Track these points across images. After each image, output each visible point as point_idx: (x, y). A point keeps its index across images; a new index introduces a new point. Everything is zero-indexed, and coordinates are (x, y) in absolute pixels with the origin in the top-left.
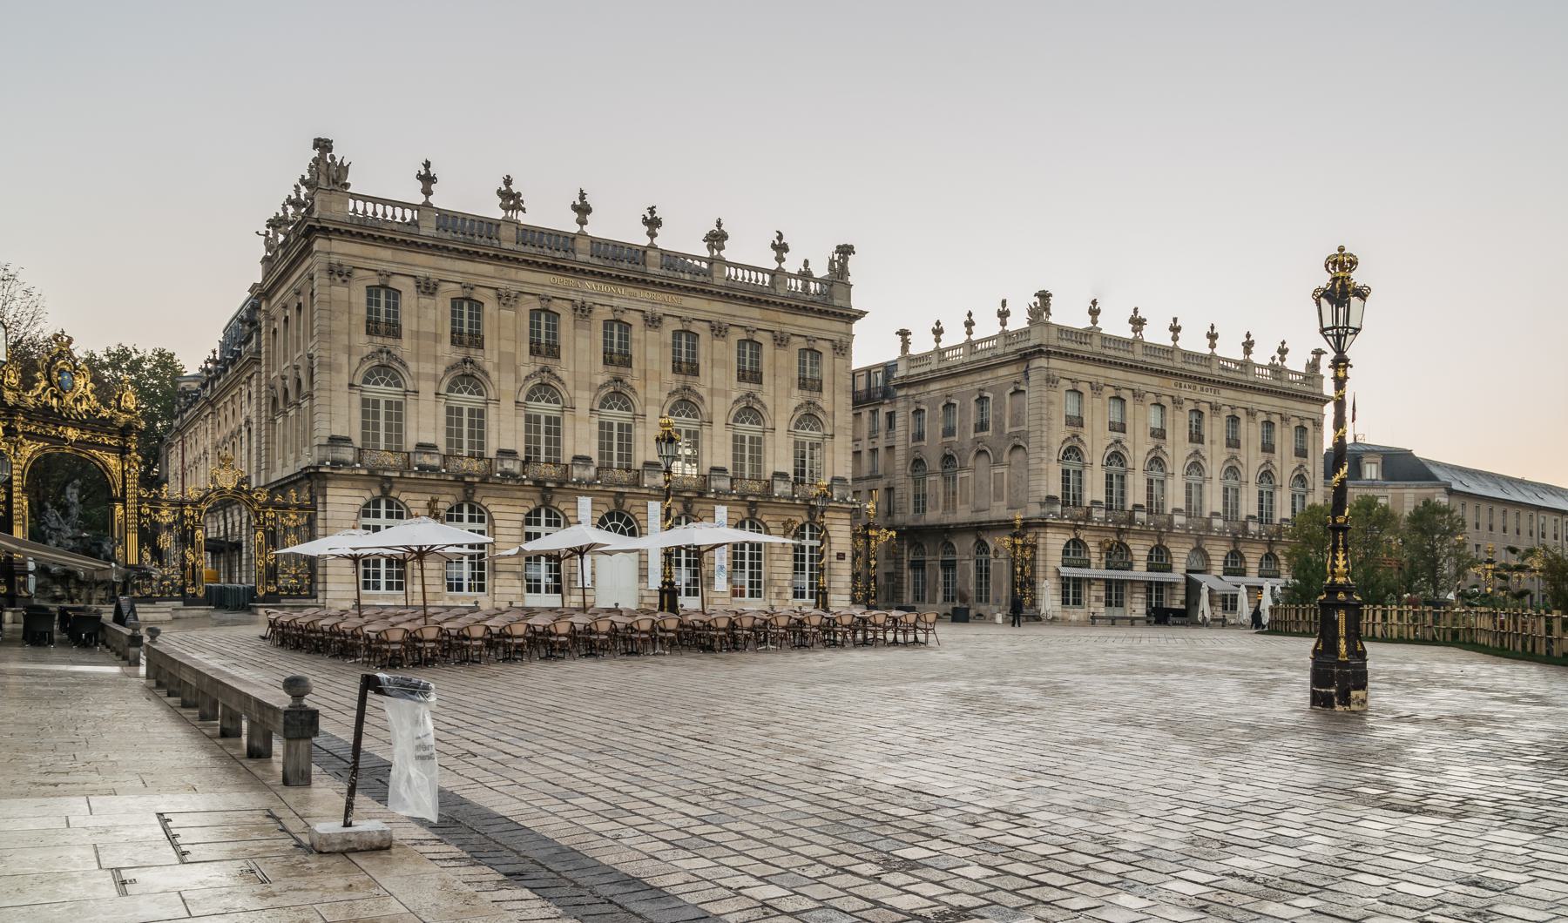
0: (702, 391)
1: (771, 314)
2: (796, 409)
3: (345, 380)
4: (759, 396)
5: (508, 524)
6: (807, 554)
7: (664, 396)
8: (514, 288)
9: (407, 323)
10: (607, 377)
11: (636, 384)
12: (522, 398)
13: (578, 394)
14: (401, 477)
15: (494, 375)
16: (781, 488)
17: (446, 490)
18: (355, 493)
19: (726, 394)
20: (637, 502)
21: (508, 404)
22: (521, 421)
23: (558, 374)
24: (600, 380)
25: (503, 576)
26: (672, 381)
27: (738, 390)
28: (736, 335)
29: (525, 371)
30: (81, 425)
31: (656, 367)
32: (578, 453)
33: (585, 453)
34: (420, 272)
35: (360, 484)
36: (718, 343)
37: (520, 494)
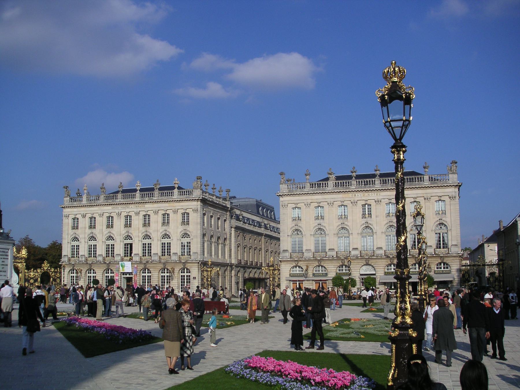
1: (172, 204)
2: (181, 232)
4: (168, 230)
6: (186, 278)
7: (140, 234)
9: (80, 226)
10: (125, 231)
12: (104, 240)
15: (98, 235)
21: (101, 242)
28: (161, 212)
34: (82, 213)
36: (156, 216)
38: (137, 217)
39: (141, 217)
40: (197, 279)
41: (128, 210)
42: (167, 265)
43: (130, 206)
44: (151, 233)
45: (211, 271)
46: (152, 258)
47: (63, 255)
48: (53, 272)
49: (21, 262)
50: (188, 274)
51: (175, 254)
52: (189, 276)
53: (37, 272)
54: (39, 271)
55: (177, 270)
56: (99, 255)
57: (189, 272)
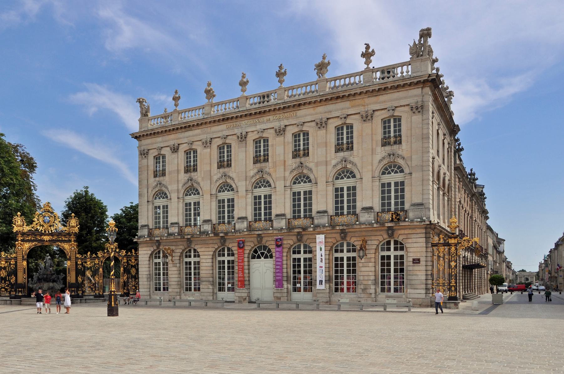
0: (311, 165)
3: (146, 199)
5: (206, 257)
7: (287, 174)
8: (208, 137)
10: (256, 171)
11: (271, 171)
12: (214, 192)
13: (239, 184)
14: (161, 239)
16: (365, 217)
17: (181, 243)
18: (148, 249)
19: (326, 163)
20: (270, 239)
21: (207, 197)
22: (214, 205)
23: (231, 175)
24: (252, 173)
25: (204, 283)
26: (292, 163)
27: (335, 158)
29: (215, 178)
30: (49, 235)
31: (282, 158)
32: (240, 216)
33: (244, 215)
35: (150, 245)
37: (211, 242)
38: (281, 139)
39: (289, 137)
40: (423, 263)
41: (260, 127)
42: (349, 235)
43: (265, 119)
44: (310, 170)
45: (456, 245)
46: (316, 222)
47: (140, 224)
48: (123, 257)
49: (70, 241)
50: (399, 253)
51: (368, 209)
52: (402, 257)
53: (98, 257)
55: (373, 243)
56: (205, 221)
57: (402, 249)
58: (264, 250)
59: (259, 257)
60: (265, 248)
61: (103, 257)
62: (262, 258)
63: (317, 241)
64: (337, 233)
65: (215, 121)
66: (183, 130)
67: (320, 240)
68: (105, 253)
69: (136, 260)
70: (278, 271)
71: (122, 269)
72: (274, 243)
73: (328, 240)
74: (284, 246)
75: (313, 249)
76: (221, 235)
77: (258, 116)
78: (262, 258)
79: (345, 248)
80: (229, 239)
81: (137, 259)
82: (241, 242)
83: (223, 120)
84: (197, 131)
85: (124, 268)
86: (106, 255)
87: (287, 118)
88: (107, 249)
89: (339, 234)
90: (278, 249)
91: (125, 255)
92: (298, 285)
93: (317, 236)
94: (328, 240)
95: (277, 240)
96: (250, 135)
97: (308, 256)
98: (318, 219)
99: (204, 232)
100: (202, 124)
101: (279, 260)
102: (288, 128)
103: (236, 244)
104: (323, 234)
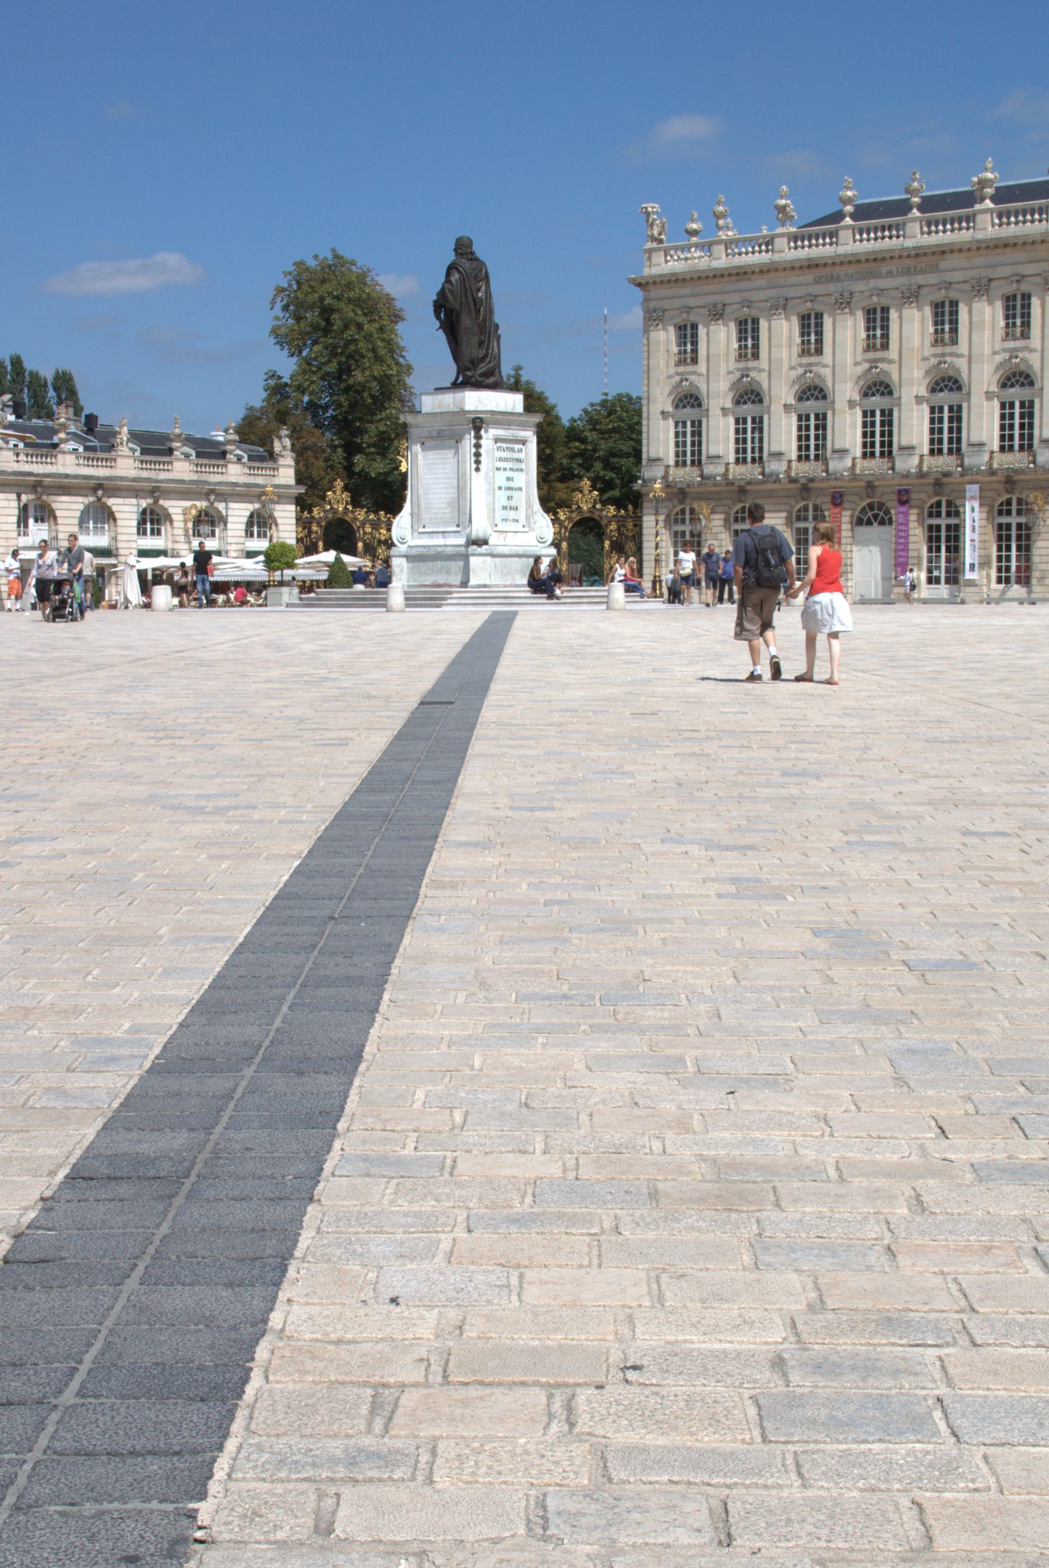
14: (688, 486)
34: (711, 299)
46: (967, 461)
47: (644, 456)
54: (562, 518)
58: (880, 509)
59: (869, 523)
60: (881, 506)
61: (569, 519)
62: (876, 524)
63: (968, 495)
64: (1000, 482)
65: (793, 268)
66: (733, 278)
67: (972, 494)
68: (572, 512)
69: (635, 525)
70: (900, 547)
71: (607, 544)
72: (894, 497)
73: (985, 494)
74: (912, 503)
75: (961, 510)
76: (803, 481)
77: (872, 265)
78: (876, 524)
79: (1014, 508)
80: (817, 489)
81: (638, 525)
82: (837, 495)
83: (809, 267)
84: (761, 282)
85: (612, 542)
86: (574, 515)
87: (923, 272)
88: (577, 504)
89: (1002, 485)
90: (902, 509)
91: (614, 516)
92: (935, 573)
93: (968, 487)
94: (985, 494)
95: (900, 492)
96: (857, 297)
97: (952, 521)
98: (969, 457)
99: (771, 475)
100: (768, 271)
101: (903, 528)
102: (923, 291)
103: (829, 499)
104: (976, 483)
